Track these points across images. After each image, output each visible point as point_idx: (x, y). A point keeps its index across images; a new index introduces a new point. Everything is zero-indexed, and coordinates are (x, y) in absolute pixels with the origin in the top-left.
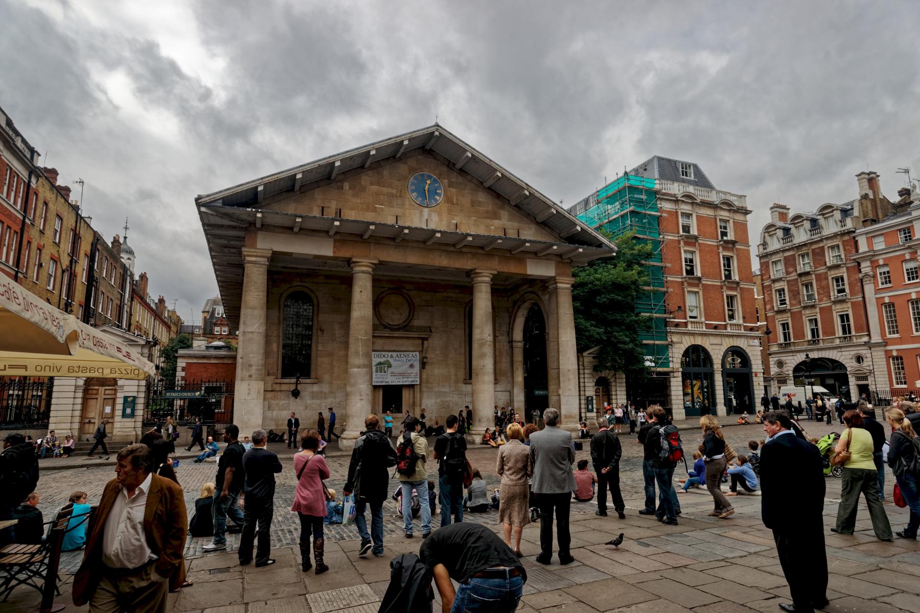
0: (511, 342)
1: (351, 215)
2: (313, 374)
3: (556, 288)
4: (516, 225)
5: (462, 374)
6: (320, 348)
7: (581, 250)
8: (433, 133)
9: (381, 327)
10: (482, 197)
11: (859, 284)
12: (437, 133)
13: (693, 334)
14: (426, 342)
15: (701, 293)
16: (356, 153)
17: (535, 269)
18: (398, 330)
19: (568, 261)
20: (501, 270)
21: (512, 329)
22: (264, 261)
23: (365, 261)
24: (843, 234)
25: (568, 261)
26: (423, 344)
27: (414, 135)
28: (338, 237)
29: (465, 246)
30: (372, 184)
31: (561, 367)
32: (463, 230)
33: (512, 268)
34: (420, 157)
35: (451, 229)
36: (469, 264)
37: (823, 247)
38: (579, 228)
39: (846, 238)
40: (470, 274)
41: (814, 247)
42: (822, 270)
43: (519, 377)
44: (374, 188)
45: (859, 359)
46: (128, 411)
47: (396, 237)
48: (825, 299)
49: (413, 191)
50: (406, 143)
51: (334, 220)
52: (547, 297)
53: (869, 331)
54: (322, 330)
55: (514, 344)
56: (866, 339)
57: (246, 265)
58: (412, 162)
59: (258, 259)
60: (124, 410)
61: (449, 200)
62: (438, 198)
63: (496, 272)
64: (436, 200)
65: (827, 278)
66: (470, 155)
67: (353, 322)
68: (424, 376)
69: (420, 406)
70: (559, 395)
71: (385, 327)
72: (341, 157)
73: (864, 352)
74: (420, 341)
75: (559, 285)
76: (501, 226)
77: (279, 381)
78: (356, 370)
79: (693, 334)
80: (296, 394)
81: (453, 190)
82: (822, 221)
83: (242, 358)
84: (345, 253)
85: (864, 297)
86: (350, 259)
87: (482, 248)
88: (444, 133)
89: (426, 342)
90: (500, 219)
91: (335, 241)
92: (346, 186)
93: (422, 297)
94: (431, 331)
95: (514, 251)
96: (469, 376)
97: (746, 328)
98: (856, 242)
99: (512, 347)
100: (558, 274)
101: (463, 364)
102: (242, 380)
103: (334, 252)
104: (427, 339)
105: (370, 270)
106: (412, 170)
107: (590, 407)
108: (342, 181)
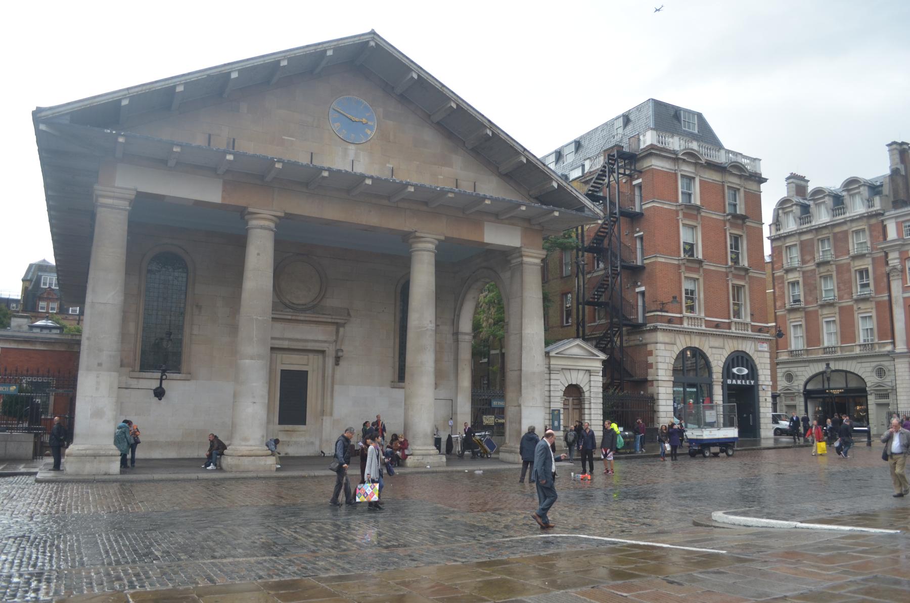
0: (456, 334)
1: (249, 147)
2: (184, 367)
3: (522, 263)
5: (390, 373)
6: (195, 332)
7: (556, 214)
8: (368, 42)
9: (284, 306)
11: (885, 280)
12: (372, 44)
13: (689, 333)
14: (341, 330)
15: (701, 280)
16: (260, 62)
17: (498, 236)
18: (304, 311)
19: (537, 227)
20: (450, 235)
21: (459, 316)
22: (125, 204)
23: (266, 213)
24: (870, 216)
25: (537, 227)
26: (337, 332)
27: (342, 44)
29: (403, 200)
31: (523, 368)
32: (400, 177)
33: (465, 233)
35: (385, 175)
37: (846, 232)
38: (555, 185)
39: (873, 221)
40: (407, 239)
41: (837, 230)
42: (844, 259)
43: (466, 382)
45: (881, 372)
47: (310, 181)
48: (846, 296)
50: (330, 53)
51: (226, 152)
52: (508, 274)
53: (893, 337)
54: (199, 307)
55: (461, 337)
56: (889, 348)
57: (99, 210)
59: (116, 202)
62: (369, 132)
63: (442, 238)
64: (366, 135)
65: (849, 271)
66: (415, 76)
67: (245, 295)
68: (338, 376)
69: (331, 415)
70: (520, 406)
71: (287, 306)
72: (239, 66)
73: (886, 364)
74: (333, 328)
75: (525, 259)
76: (456, 174)
77: (137, 374)
78: (247, 361)
79: (689, 333)
80: (159, 393)
82: (847, 199)
83: (88, 339)
84: (237, 200)
85: (890, 296)
86: (245, 208)
87: (426, 203)
88: (382, 44)
89: (341, 330)
93: (341, 267)
94: (349, 314)
95: (471, 209)
96: (401, 375)
97: (754, 329)
98: (884, 228)
99: (457, 341)
102: (88, 369)
103: (223, 198)
104: (343, 325)
105: (272, 225)
107: (556, 423)
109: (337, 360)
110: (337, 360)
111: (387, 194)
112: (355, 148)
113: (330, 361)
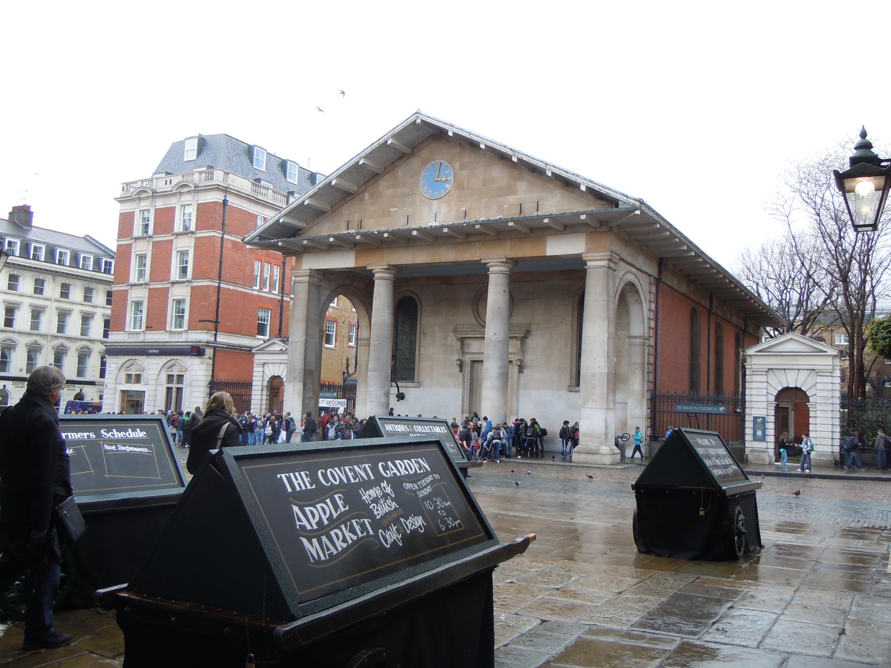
2: (416, 380)
4: (535, 196)
5: (566, 380)
6: (422, 352)
10: (498, 173)
12: (419, 121)
28: (358, 248)
30: (388, 188)
33: (527, 251)
34: (432, 145)
36: (478, 254)
44: (390, 191)
46: (759, 433)
49: (423, 186)
58: (425, 153)
60: (754, 434)
61: (459, 186)
68: (522, 382)
81: (465, 172)
90: (516, 193)
91: (356, 252)
92: (367, 195)
95: (535, 229)
96: (576, 381)
100: (589, 250)
101: (568, 367)
106: (425, 162)
108: (362, 192)
109: (521, 369)
110: (521, 369)
111: (463, 235)
112: (432, 204)
113: (516, 369)
